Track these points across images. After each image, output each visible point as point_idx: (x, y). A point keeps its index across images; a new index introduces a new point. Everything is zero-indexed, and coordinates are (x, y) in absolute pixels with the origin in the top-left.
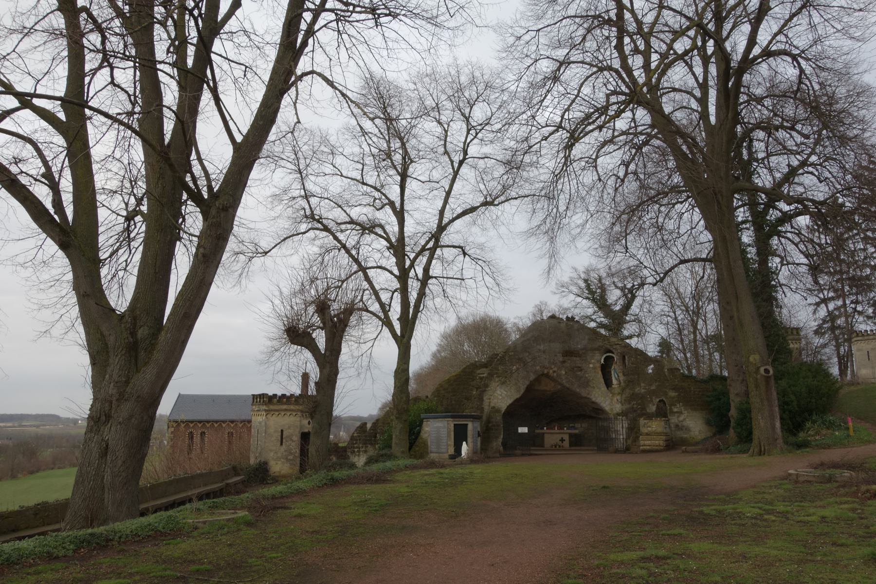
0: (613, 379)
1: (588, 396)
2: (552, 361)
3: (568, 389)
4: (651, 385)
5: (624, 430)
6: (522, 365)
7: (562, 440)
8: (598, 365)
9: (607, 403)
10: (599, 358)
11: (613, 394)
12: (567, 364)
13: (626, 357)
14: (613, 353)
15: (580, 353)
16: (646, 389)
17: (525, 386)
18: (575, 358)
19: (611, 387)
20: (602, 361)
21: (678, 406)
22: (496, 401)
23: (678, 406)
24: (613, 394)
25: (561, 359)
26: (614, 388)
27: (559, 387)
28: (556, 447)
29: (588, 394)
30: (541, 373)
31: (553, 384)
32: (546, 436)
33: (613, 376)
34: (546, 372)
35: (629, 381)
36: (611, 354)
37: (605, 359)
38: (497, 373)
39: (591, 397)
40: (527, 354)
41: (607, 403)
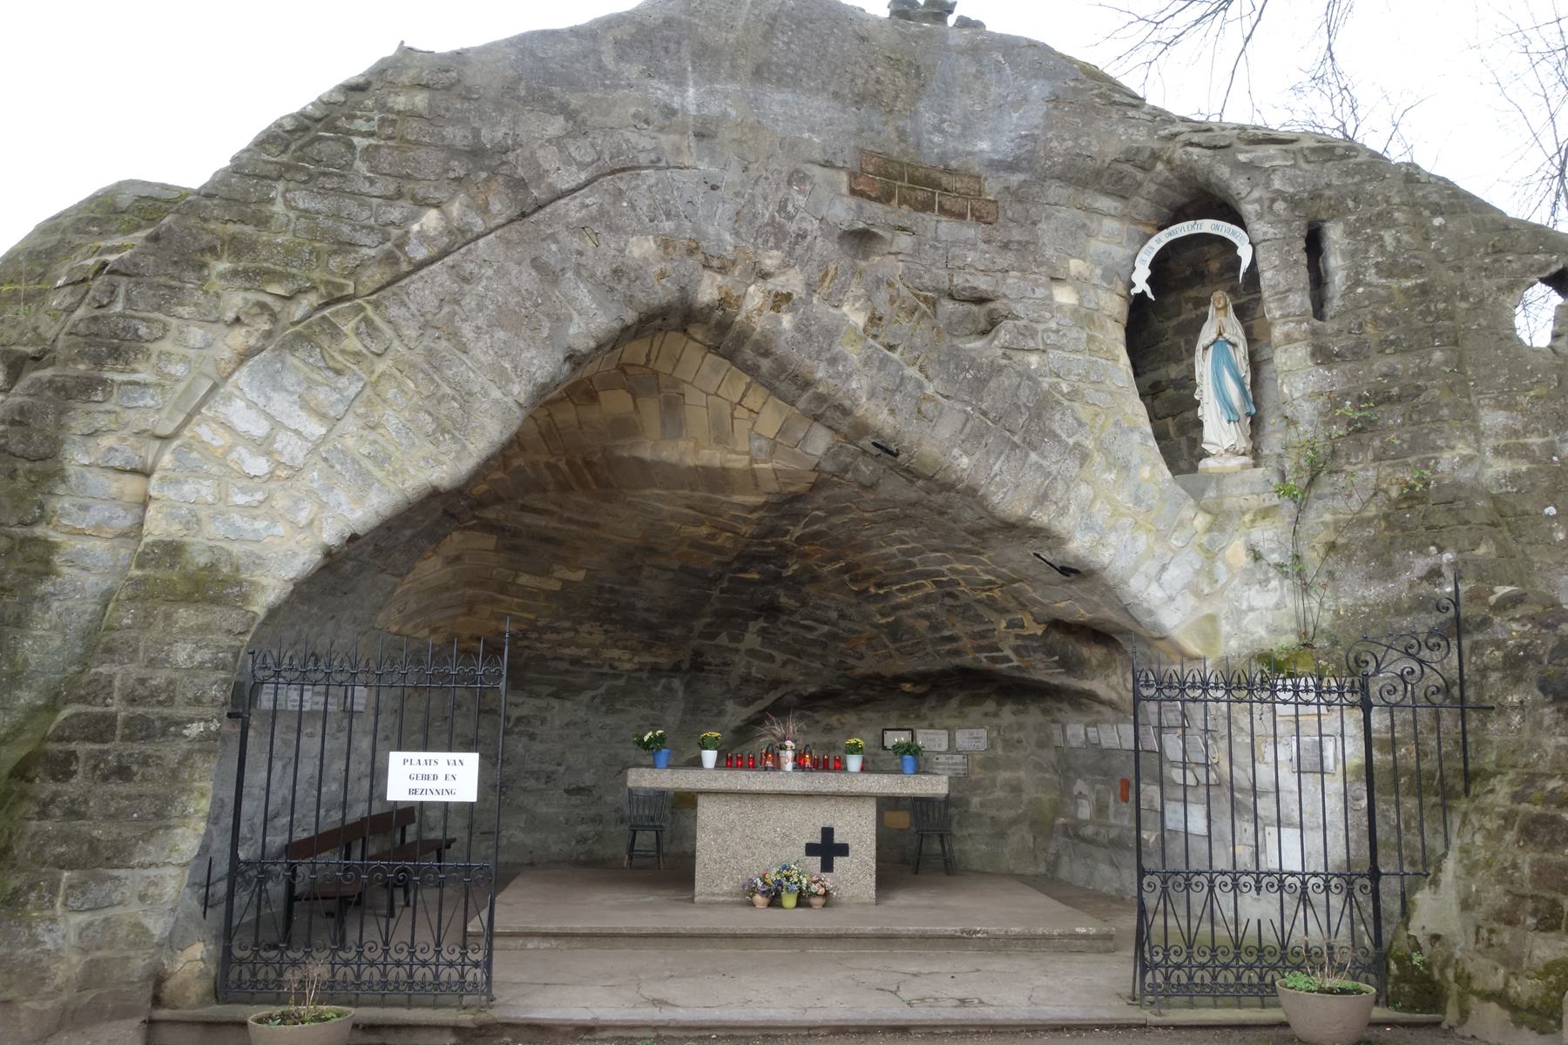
0: (1210, 413)
1: (1042, 517)
2: (766, 212)
3: (886, 451)
5: (1334, 785)
6: (500, 207)
7: (827, 849)
8: (1115, 306)
9: (1176, 574)
10: (1120, 253)
11: (1220, 519)
12: (882, 264)
13: (1335, 234)
14: (1237, 219)
15: (992, 188)
16: (1524, 452)
17: (520, 390)
18: (947, 228)
19: (1194, 469)
20: (1141, 280)
22: (207, 490)
24: (1220, 519)
25: (843, 211)
26: (1220, 478)
27: (820, 442)
28: (775, 901)
29: (1042, 499)
30: (662, 293)
31: (770, 420)
32: (707, 812)
34: (708, 291)
35: (1384, 399)
36: (1207, 226)
37: (1158, 264)
38: (237, 246)
39: (1062, 525)
40: (557, 125)
41: (1176, 574)
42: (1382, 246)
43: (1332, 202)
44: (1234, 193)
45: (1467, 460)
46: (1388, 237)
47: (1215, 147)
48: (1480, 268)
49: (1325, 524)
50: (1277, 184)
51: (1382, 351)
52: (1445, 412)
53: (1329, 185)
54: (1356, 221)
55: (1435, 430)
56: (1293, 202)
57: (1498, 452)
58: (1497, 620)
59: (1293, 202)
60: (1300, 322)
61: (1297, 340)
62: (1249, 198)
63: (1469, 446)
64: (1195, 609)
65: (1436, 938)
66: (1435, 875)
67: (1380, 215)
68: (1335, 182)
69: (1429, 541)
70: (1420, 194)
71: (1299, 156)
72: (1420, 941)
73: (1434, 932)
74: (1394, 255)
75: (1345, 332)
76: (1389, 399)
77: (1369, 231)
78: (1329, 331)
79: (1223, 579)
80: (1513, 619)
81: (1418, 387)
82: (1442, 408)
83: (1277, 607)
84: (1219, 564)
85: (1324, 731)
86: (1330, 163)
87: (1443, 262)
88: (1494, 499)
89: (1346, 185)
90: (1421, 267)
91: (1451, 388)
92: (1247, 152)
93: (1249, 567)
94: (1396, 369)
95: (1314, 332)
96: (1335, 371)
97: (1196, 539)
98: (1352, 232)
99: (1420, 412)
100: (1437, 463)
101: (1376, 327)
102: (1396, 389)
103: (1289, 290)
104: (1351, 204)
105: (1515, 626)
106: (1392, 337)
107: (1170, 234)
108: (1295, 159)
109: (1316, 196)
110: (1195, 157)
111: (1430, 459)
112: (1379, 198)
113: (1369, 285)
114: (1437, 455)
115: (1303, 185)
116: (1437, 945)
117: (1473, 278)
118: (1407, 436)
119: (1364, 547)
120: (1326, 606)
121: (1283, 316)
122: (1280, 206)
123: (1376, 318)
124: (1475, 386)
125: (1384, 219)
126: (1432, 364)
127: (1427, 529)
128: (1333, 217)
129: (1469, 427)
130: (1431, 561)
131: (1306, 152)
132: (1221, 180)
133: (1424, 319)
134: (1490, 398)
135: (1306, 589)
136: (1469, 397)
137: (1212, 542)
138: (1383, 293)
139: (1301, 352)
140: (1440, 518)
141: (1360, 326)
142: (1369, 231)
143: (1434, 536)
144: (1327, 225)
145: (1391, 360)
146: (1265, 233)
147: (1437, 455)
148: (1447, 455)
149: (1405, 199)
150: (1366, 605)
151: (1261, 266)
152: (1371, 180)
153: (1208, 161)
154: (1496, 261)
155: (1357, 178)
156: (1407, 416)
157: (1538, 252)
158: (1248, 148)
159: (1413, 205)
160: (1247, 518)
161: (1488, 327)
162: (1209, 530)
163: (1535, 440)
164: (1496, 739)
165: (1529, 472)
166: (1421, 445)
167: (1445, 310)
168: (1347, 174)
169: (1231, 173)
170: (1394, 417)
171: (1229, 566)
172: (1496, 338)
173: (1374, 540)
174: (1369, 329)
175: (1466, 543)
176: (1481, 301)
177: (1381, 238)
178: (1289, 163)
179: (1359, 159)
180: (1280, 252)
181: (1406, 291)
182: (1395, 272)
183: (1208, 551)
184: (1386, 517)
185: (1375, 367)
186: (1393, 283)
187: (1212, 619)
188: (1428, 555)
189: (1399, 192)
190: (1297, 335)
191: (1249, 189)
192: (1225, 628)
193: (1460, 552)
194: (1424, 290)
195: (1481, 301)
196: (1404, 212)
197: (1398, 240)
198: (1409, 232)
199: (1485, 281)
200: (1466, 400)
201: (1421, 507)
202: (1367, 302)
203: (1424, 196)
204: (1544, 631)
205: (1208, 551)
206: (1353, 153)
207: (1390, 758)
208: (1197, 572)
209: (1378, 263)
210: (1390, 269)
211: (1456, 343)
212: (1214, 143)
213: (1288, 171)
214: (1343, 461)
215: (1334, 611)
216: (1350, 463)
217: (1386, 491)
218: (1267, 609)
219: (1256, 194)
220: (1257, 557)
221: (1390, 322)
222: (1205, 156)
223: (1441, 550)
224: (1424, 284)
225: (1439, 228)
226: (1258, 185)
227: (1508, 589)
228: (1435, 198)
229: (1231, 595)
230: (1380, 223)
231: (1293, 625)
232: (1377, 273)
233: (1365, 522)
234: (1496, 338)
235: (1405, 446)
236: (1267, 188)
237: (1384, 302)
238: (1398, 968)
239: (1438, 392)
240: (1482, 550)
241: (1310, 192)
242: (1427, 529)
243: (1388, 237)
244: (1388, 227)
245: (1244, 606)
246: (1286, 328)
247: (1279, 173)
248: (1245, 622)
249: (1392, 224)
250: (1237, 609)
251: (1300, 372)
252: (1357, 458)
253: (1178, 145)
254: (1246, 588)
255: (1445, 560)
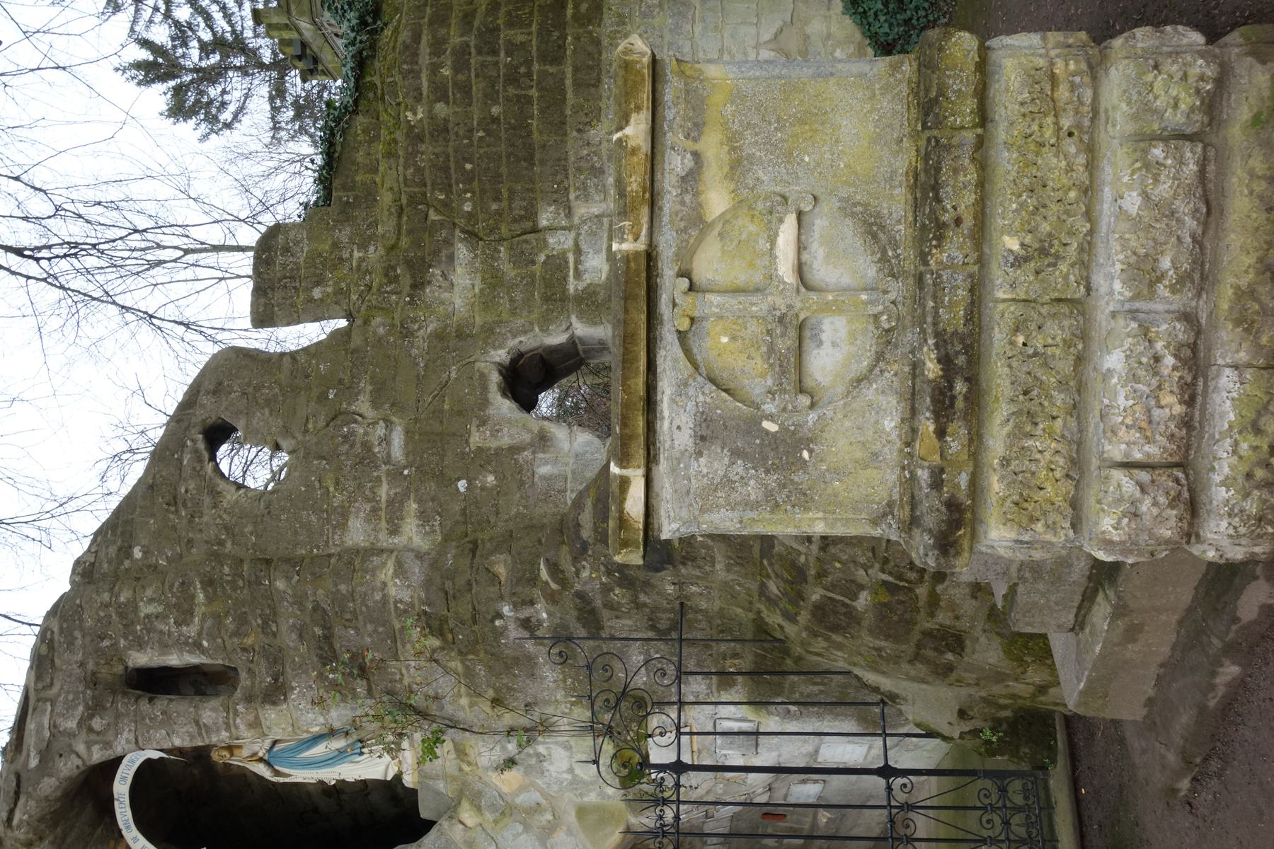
4: (367, 459)
5: (771, 723)
13: (141, 659)
14: (115, 763)
21: (560, 242)
23: (560, 242)
33: (330, 775)
36: (121, 787)
42: (157, 617)
43: (102, 662)
44: (76, 772)
45: (400, 570)
46: (146, 609)
47: (17, 794)
48: (191, 521)
49: (471, 705)
50: (71, 724)
51: (274, 635)
52: (343, 588)
53: (82, 665)
54: (126, 638)
55: (364, 600)
56: (95, 708)
57: (394, 531)
58: (578, 587)
59: (95, 708)
60: (236, 713)
61: (257, 717)
62: (85, 757)
63: (384, 564)
64: (570, 832)
65: (962, 714)
66: (882, 694)
67: (121, 615)
68: (79, 657)
69: (490, 625)
70: (106, 566)
71: (43, 694)
72: (967, 729)
73: (956, 715)
74: (168, 606)
75: (252, 666)
76: (328, 638)
77: (138, 628)
78: (249, 683)
79: (535, 797)
80: (577, 573)
81: (315, 609)
82: (338, 590)
83: (568, 748)
84: (518, 801)
85: (710, 729)
86: (56, 660)
87: (181, 556)
88: (446, 539)
89: (84, 647)
90: (183, 583)
91: (317, 577)
92: (28, 756)
93: (522, 770)
94: (294, 625)
95: (249, 699)
96: (294, 684)
97: (488, 827)
98: (140, 645)
99: (343, 611)
100: (401, 601)
101: (247, 635)
102: (316, 629)
103: (197, 723)
104: (106, 643)
105: (585, 574)
106: (259, 621)
107: (128, 828)
108: (46, 700)
109: (93, 681)
110: (25, 817)
111: (396, 607)
112: (102, 614)
113: (200, 634)
114: (392, 600)
115: (76, 693)
116: (971, 713)
117: (201, 531)
118: (370, 627)
119: (498, 675)
120: (567, 711)
121: (228, 728)
122: (97, 723)
123: (237, 633)
124: (318, 548)
125: (127, 613)
126: (290, 591)
127: (475, 622)
128: (121, 660)
129: (363, 561)
130: (512, 626)
131: (40, 686)
132: (57, 788)
133: (242, 588)
134: (334, 533)
135: (544, 727)
136: (330, 556)
137: (493, 807)
138: (209, 623)
139: (270, 715)
140: (464, 609)
141: (244, 650)
142: (138, 628)
143: (483, 618)
144: (130, 664)
145: (284, 628)
146: (128, 741)
147: (392, 600)
148: (392, 591)
149: (106, 587)
150: (565, 681)
151: (167, 745)
152: (81, 620)
153: (32, 803)
154: (185, 505)
155: (77, 634)
156: (347, 624)
157: (180, 460)
158: (24, 753)
159: (116, 578)
160: (466, 768)
161: (255, 524)
162: (479, 809)
163: (384, 492)
164: (717, 605)
165: (420, 501)
166: (380, 614)
167: (231, 567)
168: (71, 644)
169: (50, 776)
170: (346, 637)
171: (523, 789)
172: (267, 518)
173: (490, 668)
174: (249, 641)
175: (492, 589)
176: (227, 528)
177: (148, 616)
178: (49, 708)
179: (56, 630)
180: (150, 728)
181: (210, 600)
182: (186, 607)
183: (503, 814)
184: (460, 653)
185: (291, 644)
186: (200, 610)
187: (582, 812)
188: (505, 628)
189: (98, 593)
190: (251, 717)
191: (73, 756)
192: (592, 798)
193: (502, 598)
194: (209, 583)
195: (227, 528)
196: (121, 590)
197: (151, 600)
198: (143, 587)
199: (205, 519)
200: (333, 560)
201: (451, 623)
202: (219, 640)
203: (109, 563)
204: (590, 552)
205: (503, 814)
206: (49, 636)
207: (740, 679)
208: (527, 828)
209: (175, 623)
210: (185, 613)
211: (268, 562)
212: (12, 794)
213: (58, 710)
214: (398, 685)
215: (572, 705)
216: (401, 680)
217: (434, 651)
218: (571, 757)
219: (81, 748)
220: (511, 762)
221: (242, 620)
222: (25, 806)
223: (499, 615)
224: (201, 582)
225: (145, 553)
226: (70, 745)
227: (542, 566)
228: (113, 550)
229: (555, 788)
230: (131, 616)
231: (589, 741)
232: (188, 625)
233: (469, 673)
234: (267, 518)
235: (381, 629)
236: (75, 736)
237: (220, 623)
238: (1002, 755)
239: (320, 592)
240: (501, 570)
241: (87, 687)
242: (475, 622)
243: (146, 609)
244: (136, 608)
245: (569, 777)
246: (242, 727)
247: (60, 721)
248: (586, 777)
249: (133, 605)
250: (571, 783)
251: (294, 716)
252: (395, 673)
253: (9, 833)
254: (546, 774)
255: (511, 614)
